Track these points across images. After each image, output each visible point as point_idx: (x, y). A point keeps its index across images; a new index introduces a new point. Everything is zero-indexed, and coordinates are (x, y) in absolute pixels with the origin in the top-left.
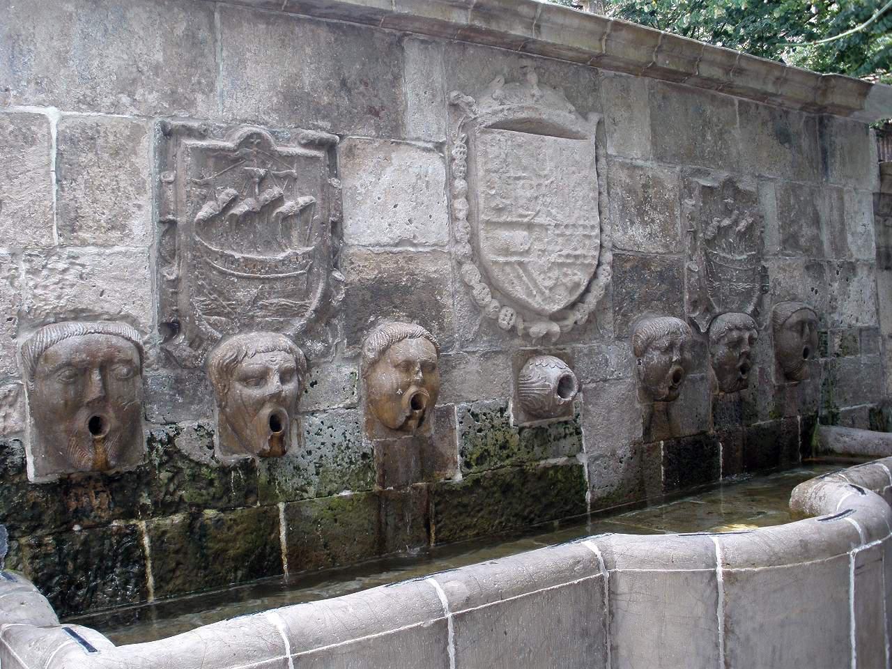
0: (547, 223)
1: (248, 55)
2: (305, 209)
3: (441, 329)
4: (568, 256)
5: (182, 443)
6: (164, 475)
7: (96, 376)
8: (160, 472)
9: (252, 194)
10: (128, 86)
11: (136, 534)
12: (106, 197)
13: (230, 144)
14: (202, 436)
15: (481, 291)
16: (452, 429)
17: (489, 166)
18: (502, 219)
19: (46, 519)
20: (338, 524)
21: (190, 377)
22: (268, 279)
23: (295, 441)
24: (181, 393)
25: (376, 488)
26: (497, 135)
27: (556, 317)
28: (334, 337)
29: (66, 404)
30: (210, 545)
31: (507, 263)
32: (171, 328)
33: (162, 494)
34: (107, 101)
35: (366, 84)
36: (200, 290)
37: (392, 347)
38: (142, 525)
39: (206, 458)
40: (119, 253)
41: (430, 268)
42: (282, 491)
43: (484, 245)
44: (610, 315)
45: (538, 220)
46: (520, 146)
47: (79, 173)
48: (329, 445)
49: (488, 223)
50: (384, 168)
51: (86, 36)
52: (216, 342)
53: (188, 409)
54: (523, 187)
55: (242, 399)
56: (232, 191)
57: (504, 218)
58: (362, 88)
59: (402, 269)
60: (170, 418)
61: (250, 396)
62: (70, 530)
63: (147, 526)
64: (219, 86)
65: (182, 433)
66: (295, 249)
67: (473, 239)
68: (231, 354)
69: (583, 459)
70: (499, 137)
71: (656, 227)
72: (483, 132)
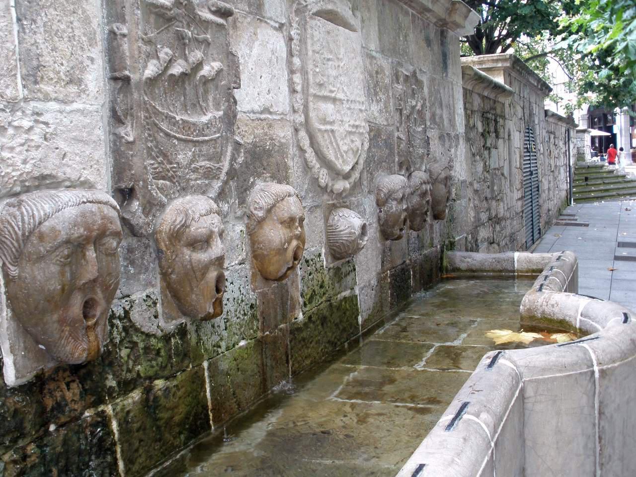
6: (124, 352)
8: (120, 350)
11: (103, 421)
14: (149, 306)
19: (28, 426)
20: (240, 373)
22: (198, 141)
25: (259, 334)
29: (63, 289)
30: (161, 415)
31: (326, 131)
32: (125, 194)
33: (124, 373)
37: (277, 205)
38: (109, 409)
39: (153, 329)
40: (78, 111)
42: (206, 350)
43: (312, 114)
47: (38, 14)
48: (231, 300)
53: (138, 280)
55: (191, 265)
61: (199, 261)
62: (47, 433)
63: (114, 410)
65: (135, 306)
68: (181, 219)
70: (319, 23)
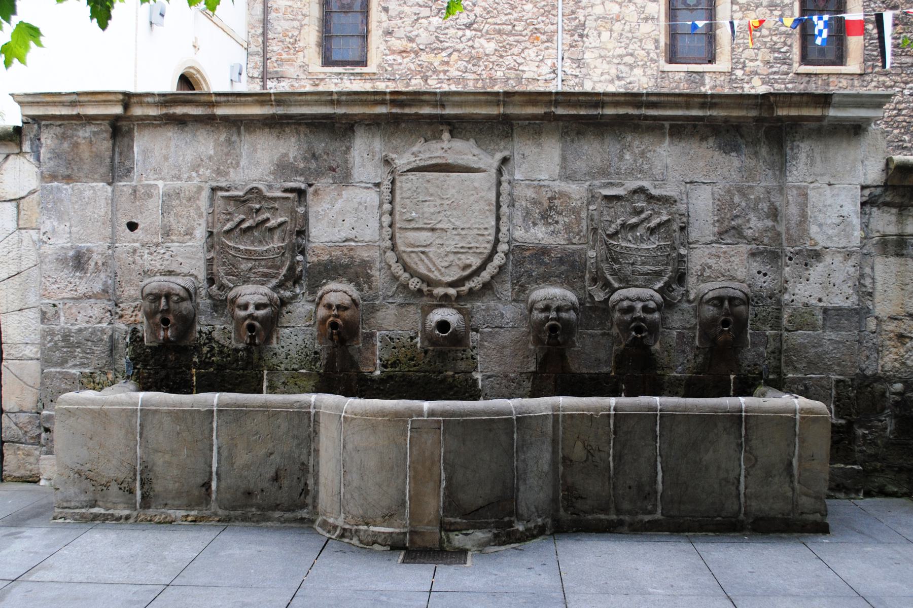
1: (259, 146)
3: (370, 288)
4: (462, 247)
5: (215, 335)
7: (163, 300)
9: (252, 218)
10: (195, 168)
12: (184, 221)
13: (241, 193)
15: (398, 269)
16: (374, 345)
17: (404, 195)
21: (221, 305)
23: (275, 340)
24: (216, 312)
26: (410, 176)
27: (452, 284)
28: (301, 290)
31: (412, 252)
32: (211, 281)
34: (185, 176)
35: (328, 154)
36: (224, 264)
39: (226, 344)
41: (365, 255)
43: (399, 241)
44: (508, 285)
45: (439, 226)
49: (400, 228)
50: (336, 200)
51: (177, 146)
52: (231, 289)
54: (429, 206)
56: (242, 217)
57: (413, 225)
58: (325, 157)
59: (345, 255)
60: (210, 322)
64: (242, 164)
66: (276, 243)
67: (392, 238)
69: (478, 376)
71: (560, 226)
72: (400, 175)
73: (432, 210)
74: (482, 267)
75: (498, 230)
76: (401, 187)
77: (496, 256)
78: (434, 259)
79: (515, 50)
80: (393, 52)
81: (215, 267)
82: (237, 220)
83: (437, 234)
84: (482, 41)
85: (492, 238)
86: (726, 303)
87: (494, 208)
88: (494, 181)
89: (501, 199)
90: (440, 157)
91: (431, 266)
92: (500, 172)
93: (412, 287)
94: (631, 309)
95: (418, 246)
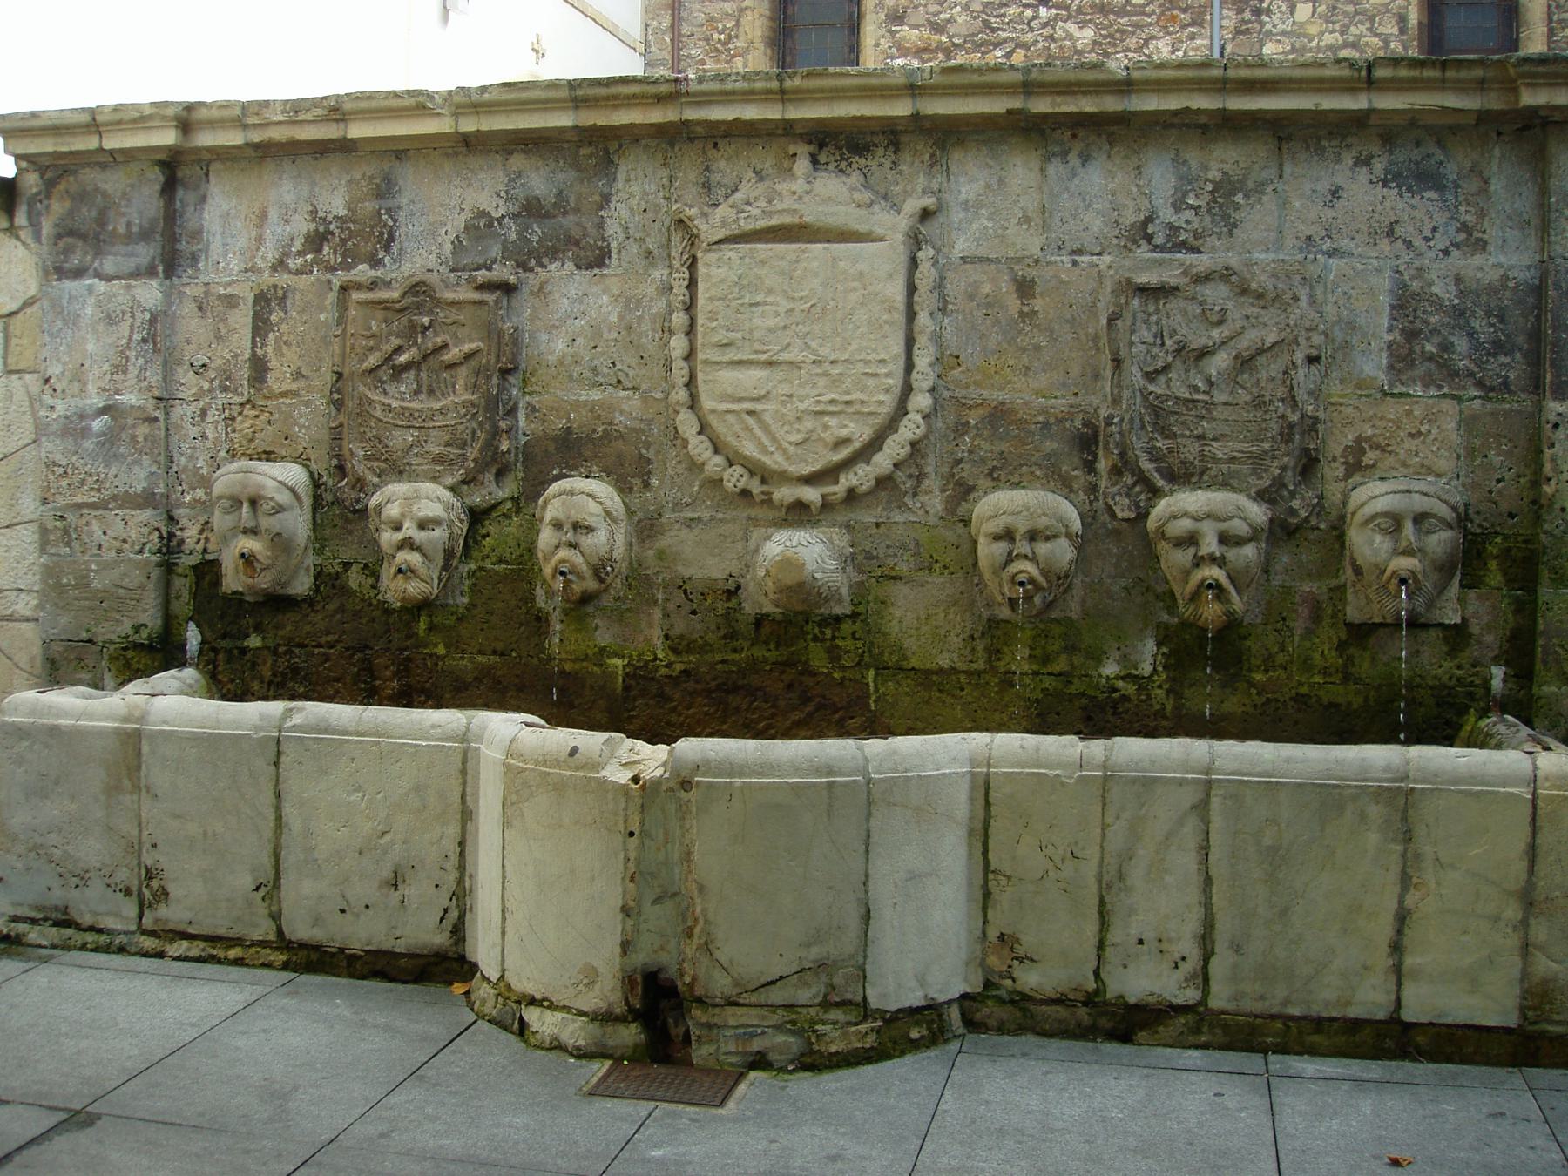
0: (800, 358)
2: (469, 356)
4: (831, 402)
7: (246, 508)
13: (396, 295)
15: (699, 447)
18: (726, 358)
26: (729, 252)
27: (810, 480)
31: (728, 412)
43: (702, 389)
45: (785, 356)
46: (763, 263)
49: (706, 362)
52: (376, 488)
54: (763, 315)
57: (731, 355)
66: (462, 395)
67: (691, 383)
73: (771, 323)
74: (874, 445)
75: (909, 366)
76: (708, 276)
77: (905, 421)
78: (773, 428)
79: (1132, 42)
80: (904, 52)
81: (345, 443)
82: (388, 348)
83: (779, 373)
84: (1071, 27)
85: (895, 382)
86: (1409, 527)
87: (900, 317)
88: (903, 259)
89: (916, 298)
90: (788, 211)
91: (767, 442)
92: (915, 241)
93: (729, 486)
94: (1191, 540)
95: (740, 400)
